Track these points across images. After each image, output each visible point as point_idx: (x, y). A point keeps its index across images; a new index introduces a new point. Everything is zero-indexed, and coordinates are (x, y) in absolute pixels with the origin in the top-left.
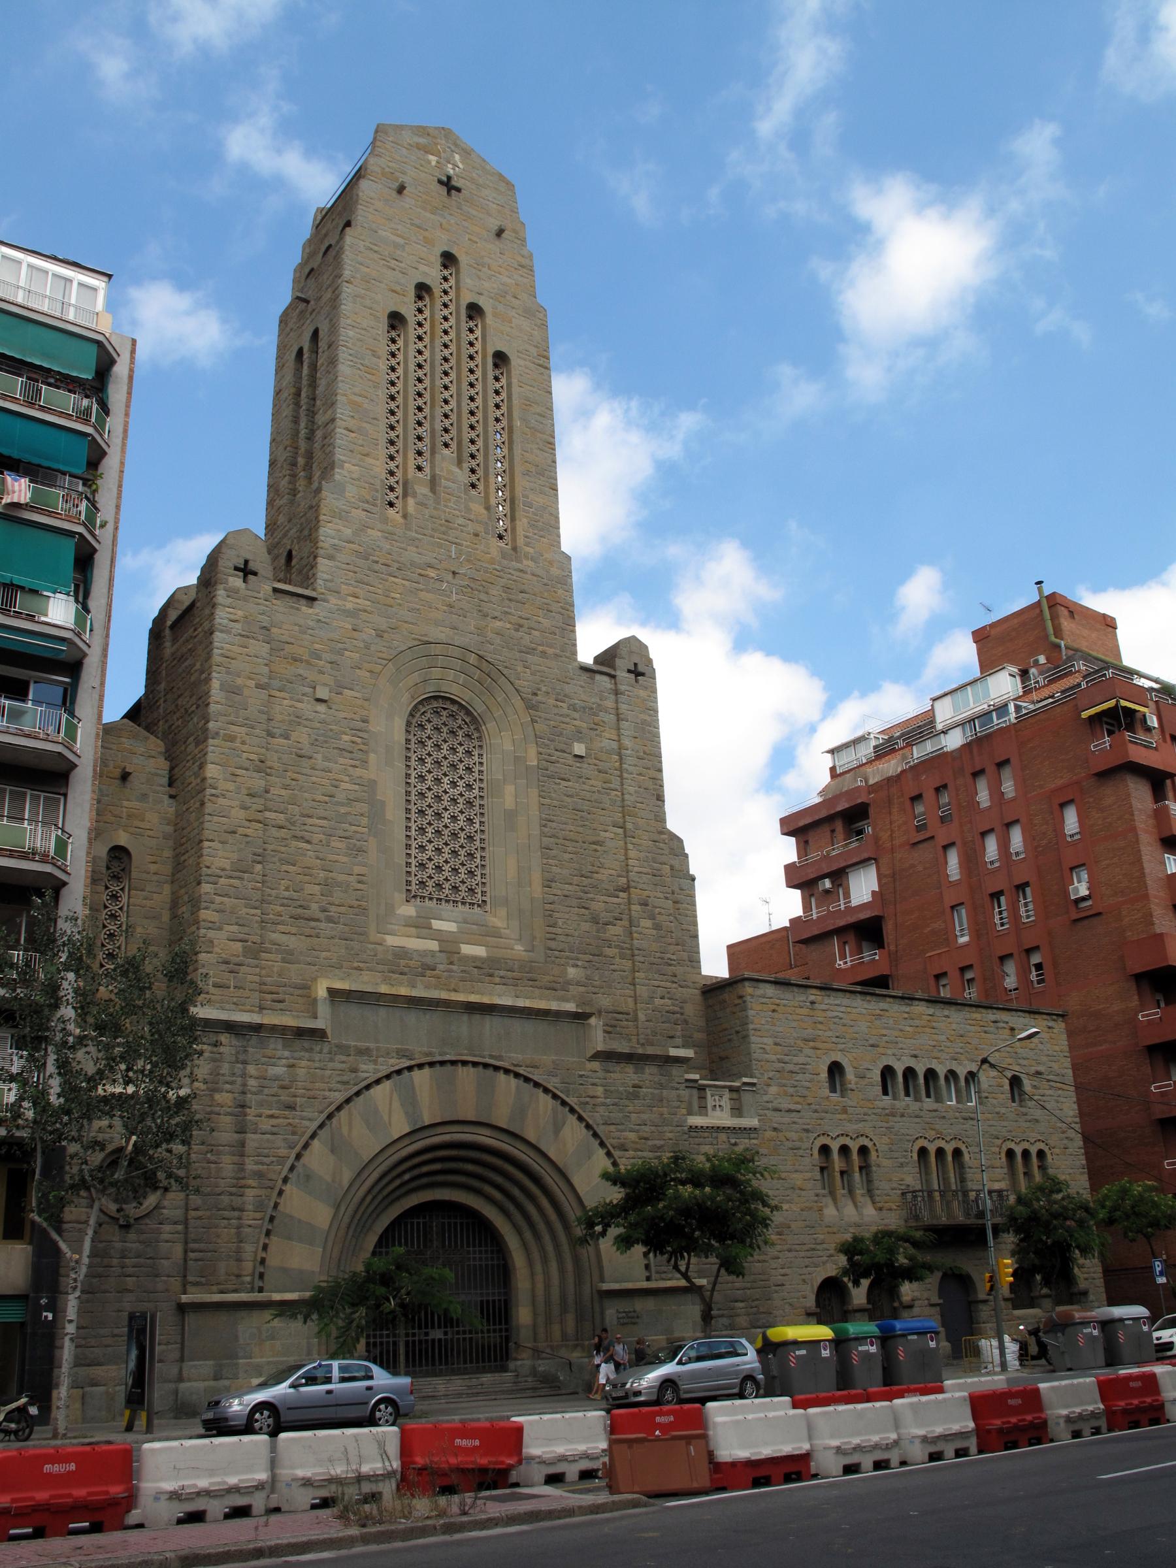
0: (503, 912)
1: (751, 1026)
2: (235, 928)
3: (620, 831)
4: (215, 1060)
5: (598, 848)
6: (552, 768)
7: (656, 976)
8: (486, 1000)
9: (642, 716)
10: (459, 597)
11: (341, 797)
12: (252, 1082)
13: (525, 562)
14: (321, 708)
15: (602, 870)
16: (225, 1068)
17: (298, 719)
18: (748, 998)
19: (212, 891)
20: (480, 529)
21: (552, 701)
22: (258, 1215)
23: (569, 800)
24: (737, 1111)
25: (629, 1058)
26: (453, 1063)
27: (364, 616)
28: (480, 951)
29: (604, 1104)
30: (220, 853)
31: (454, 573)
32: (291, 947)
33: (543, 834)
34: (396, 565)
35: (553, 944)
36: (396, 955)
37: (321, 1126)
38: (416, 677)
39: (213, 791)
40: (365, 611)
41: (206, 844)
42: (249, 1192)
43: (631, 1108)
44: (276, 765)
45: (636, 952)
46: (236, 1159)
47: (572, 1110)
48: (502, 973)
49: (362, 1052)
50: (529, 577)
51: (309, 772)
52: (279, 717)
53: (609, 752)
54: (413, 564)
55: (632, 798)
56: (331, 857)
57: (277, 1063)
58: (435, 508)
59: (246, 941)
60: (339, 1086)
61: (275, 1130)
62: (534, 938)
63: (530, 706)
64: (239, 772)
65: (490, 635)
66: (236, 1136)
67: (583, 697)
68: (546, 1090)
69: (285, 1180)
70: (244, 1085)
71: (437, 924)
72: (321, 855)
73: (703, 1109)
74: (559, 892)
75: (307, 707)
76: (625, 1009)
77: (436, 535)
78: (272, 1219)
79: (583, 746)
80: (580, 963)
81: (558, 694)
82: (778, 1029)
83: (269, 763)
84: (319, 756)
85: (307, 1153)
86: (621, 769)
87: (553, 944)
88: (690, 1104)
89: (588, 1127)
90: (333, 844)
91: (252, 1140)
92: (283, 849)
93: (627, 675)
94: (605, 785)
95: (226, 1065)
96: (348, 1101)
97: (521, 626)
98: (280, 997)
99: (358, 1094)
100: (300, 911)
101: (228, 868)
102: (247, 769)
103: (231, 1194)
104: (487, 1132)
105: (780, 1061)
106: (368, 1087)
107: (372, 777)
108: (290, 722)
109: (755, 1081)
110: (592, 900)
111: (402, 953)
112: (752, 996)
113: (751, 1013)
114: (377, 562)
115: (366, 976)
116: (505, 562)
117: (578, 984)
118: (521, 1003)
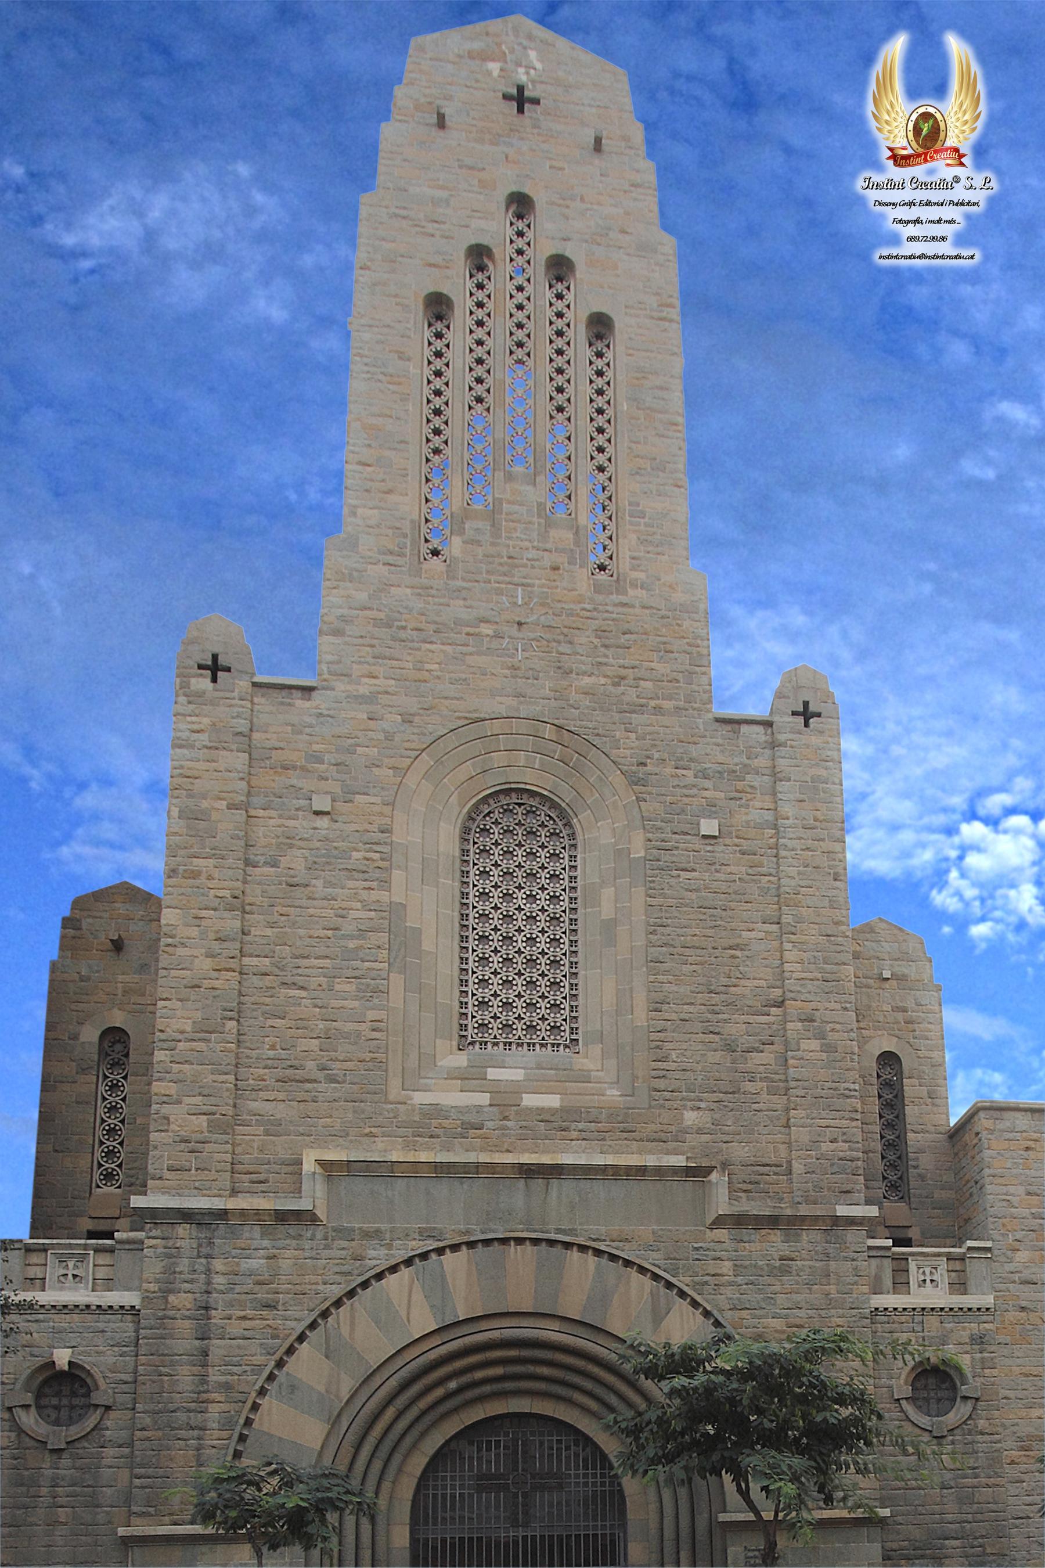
0: (597, 1049)
1: (987, 1172)
2: (198, 1099)
3: (775, 927)
4: (170, 1256)
5: (738, 953)
6: (666, 857)
7: (824, 1114)
8: (546, 1159)
9: (814, 771)
10: (526, 654)
11: (348, 928)
12: (219, 1280)
13: (631, 592)
14: (323, 822)
15: (743, 982)
16: (184, 1265)
17: (289, 841)
18: (984, 1135)
19: (168, 1060)
20: (562, 559)
21: (669, 770)
22: (225, 1434)
23: (693, 895)
24: (960, 1286)
25: (773, 1222)
26: (504, 1241)
27: (384, 699)
28: (553, 1101)
29: (731, 1284)
30: (179, 1013)
31: (520, 624)
32: (278, 1116)
33: (651, 944)
34: (433, 627)
35: (661, 1084)
36: (424, 1115)
37: (313, 1326)
38: (468, 769)
39: (170, 941)
40: (387, 693)
41: (160, 1004)
42: (212, 1407)
43: (777, 1288)
44: (258, 900)
45: (793, 1084)
46: (196, 1370)
47: (682, 1294)
48: (581, 1126)
49: (367, 1235)
50: (638, 611)
51: (304, 902)
52: (263, 841)
53: (760, 827)
54: (458, 622)
55: (793, 883)
56: (334, 1003)
57: (254, 1255)
58: (493, 544)
59: (214, 1114)
60: (338, 1278)
61: (247, 1333)
62: (635, 1078)
63: (634, 781)
64: (204, 913)
65: (574, 697)
66: (197, 1343)
67: (721, 758)
68: (642, 1270)
69: (262, 1392)
70: (209, 1283)
71: (492, 1073)
72: (319, 1002)
73: (900, 1284)
74: (674, 1016)
75: (302, 825)
76: (773, 1160)
77: (493, 578)
78: (242, 1438)
79: (715, 823)
80: (703, 1105)
81: (682, 759)
82: (1033, 1173)
83: (249, 899)
84: (319, 883)
85: (292, 1361)
86: (776, 847)
87: (661, 1084)
88: (878, 1278)
89: (707, 1314)
90: (337, 987)
91: (218, 1348)
92: (268, 1000)
93: (791, 719)
94: (750, 871)
95: (186, 1261)
96: (351, 1294)
97: (623, 678)
98: (262, 1177)
99: (365, 1285)
100: (289, 1072)
101: (189, 1029)
102: (215, 910)
103: (189, 1411)
104: (556, 1325)
105: (1034, 1216)
106: (379, 1276)
107: (396, 899)
108: (278, 845)
109: (989, 1244)
110: (725, 1021)
111: (436, 1111)
112: (991, 1131)
113: (987, 1153)
114: (404, 628)
115: (380, 1143)
116: (600, 598)
117: (700, 1131)
118: (599, 1160)
